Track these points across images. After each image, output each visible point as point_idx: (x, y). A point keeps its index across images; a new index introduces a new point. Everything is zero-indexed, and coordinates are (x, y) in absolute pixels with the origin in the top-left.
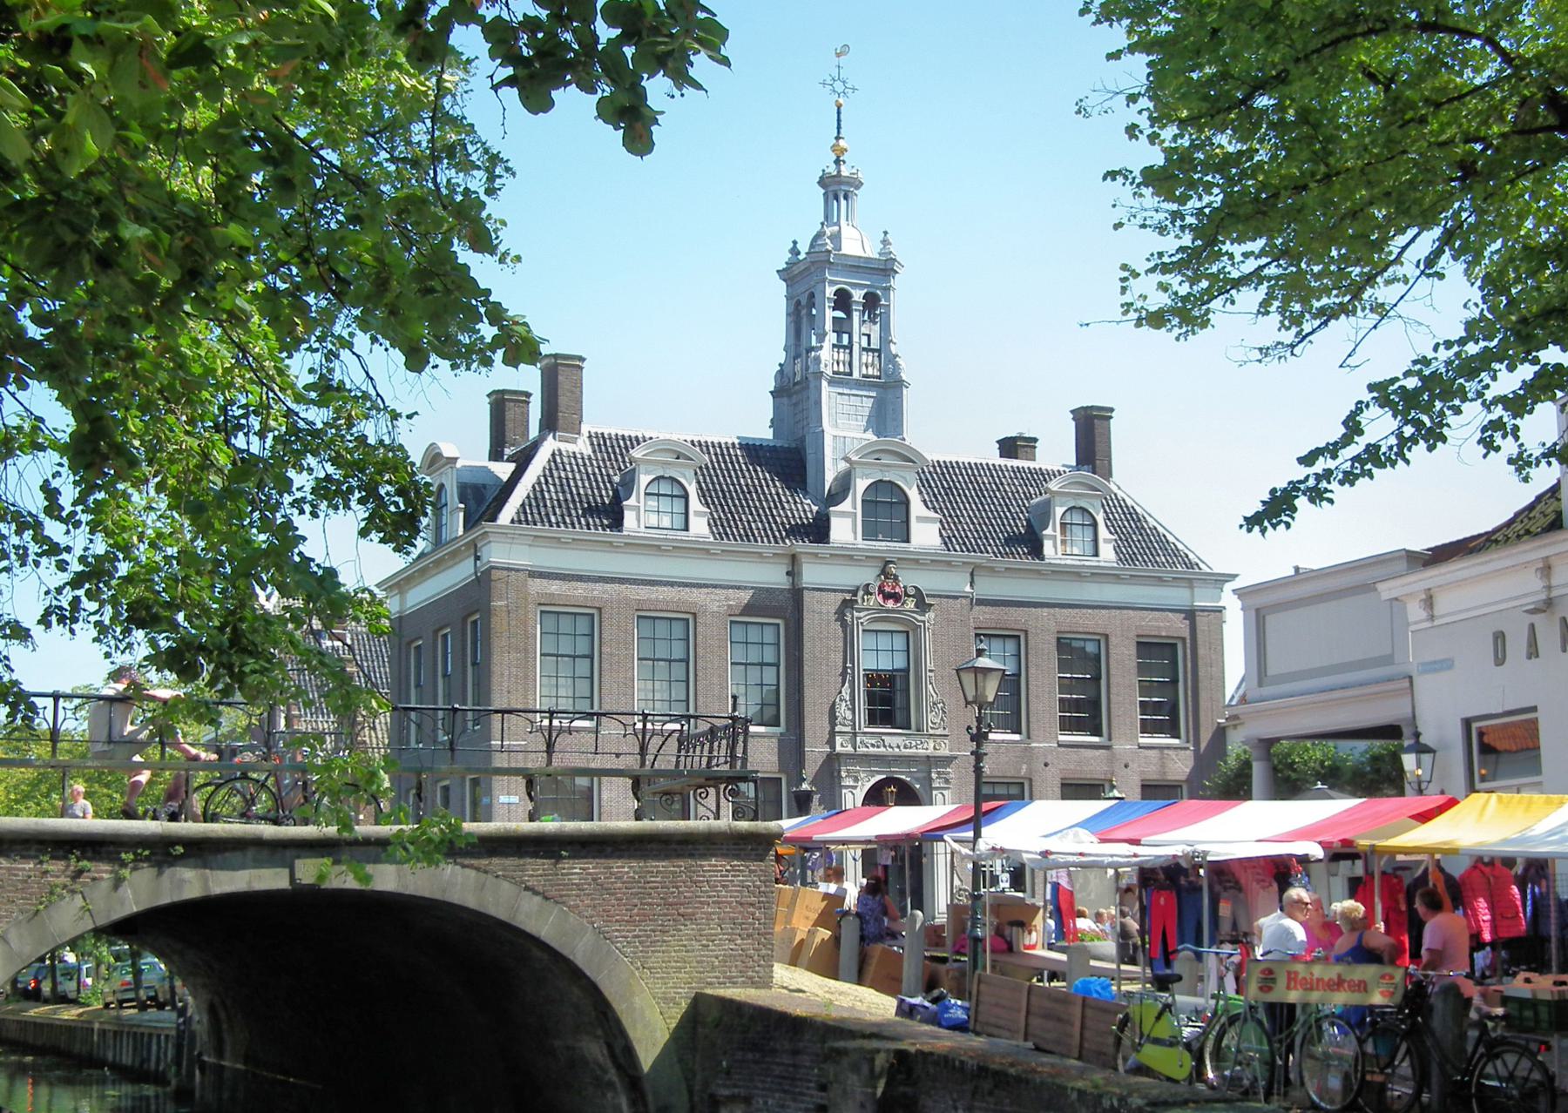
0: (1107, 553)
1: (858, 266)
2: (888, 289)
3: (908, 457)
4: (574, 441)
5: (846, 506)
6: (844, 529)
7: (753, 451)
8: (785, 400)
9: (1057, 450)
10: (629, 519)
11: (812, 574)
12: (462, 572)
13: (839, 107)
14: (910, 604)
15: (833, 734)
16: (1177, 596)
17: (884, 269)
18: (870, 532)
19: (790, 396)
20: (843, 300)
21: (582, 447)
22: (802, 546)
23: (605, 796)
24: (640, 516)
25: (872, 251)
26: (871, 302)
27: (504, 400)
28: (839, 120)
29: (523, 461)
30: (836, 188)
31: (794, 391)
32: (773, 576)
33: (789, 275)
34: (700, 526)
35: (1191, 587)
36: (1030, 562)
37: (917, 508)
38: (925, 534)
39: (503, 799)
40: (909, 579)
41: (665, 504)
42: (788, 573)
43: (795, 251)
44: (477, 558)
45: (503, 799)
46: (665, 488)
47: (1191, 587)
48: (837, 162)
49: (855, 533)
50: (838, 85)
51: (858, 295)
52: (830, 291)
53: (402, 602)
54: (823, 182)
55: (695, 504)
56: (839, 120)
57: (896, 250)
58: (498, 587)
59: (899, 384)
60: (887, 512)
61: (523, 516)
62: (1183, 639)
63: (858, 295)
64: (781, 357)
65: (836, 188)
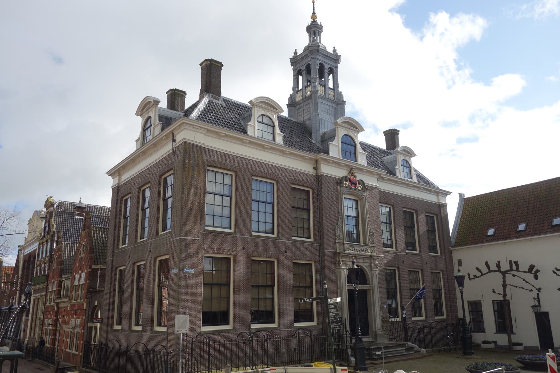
0: (415, 179)
4: (218, 99)
5: (335, 142)
8: (293, 108)
10: (250, 132)
13: (313, 2)
19: (295, 106)
20: (322, 67)
21: (220, 102)
22: (322, 156)
24: (255, 129)
27: (175, 94)
28: (314, 7)
33: (295, 61)
34: (279, 139)
35: (438, 196)
40: (359, 177)
41: (265, 127)
42: (314, 168)
43: (296, 53)
44: (174, 141)
46: (265, 120)
47: (438, 196)
49: (339, 154)
51: (327, 67)
52: (318, 62)
53: (119, 179)
55: (277, 130)
56: (314, 7)
57: (339, 52)
64: (291, 92)
65: (314, 29)
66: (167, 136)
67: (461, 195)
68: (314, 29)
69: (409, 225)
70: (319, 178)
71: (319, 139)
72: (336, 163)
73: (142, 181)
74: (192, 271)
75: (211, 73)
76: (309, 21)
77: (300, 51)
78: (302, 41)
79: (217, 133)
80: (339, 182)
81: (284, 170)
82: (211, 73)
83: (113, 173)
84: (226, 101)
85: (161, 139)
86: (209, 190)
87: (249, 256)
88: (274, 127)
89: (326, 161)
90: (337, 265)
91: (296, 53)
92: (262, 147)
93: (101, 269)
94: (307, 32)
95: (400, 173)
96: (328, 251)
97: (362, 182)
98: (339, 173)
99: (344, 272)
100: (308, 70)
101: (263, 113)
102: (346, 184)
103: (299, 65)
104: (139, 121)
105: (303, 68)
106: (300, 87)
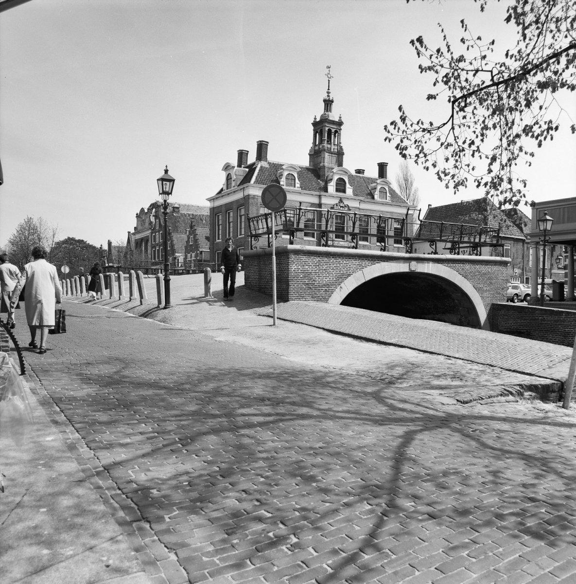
1: (333, 122)
2: (341, 129)
3: (346, 172)
6: (332, 188)
7: (307, 169)
9: (372, 172)
11: (324, 200)
12: (239, 196)
14: (346, 209)
17: (340, 123)
18: (337, 190)
20: (330, 131)
22: (323, 193)
25: (337, 119)
26: (336, 132)
29: (252, 168)
30: (328, 103)
31: (316, 154)
32: (315, 200)
33: (315, 124)
36: (372, 201)
37: (348, 185)
38: (349, 191)
40: (346, 202)
43: (315, 119)
48: (328, 96)
51: (333, 130)
52: (327, 129)
54: (325, 101)
59: (343, 154)
60: (341, 187)
61: (257, 182)
63: (333, 130)
65: (328, 103)
66: (241, 189)
75: (262, 147)
76: (325, 96)
78: (319, 111)
82: (262, 147)
84: (269, 163)
88: (295, 179)
91: (315, 119)
104: (224, 175)
105: (319, 131)
106: (317, 144)
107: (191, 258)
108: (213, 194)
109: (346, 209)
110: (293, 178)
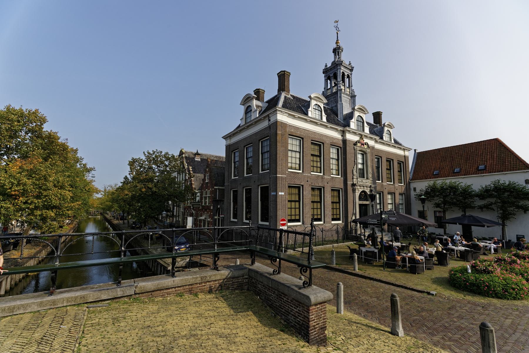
0: (393, 142)
5: (353, 120)
15: (353, 178)
16: (401, 152)
21: (289, 96)
23: (304, 193)
24: (312, 113)
34: (324, 119)
39: (280, 193)
40: (366, 140)
42: (342, 136)
43: (326, 66)
44: (269, 120)
45: (280, 193)
50: (337, 27)
51: (346, 74)
52: (342, 71)
55: (323, 113)
57: (353, 65)
58: (279, 127)
62: (403, 162)
65: (337, 51)
66: (265, 117)
67: (415, 150)
68: (337, 51)
69: (388, 168)
70: (345, 141)
71: (342, 118)
72: (355, 133)
73: (248, 142)
74: (283, 194)
75: (283, 78)
77: (329, 65)
79: (294, 116)
80: (355, 144)
81: (327, 137)
82: (283, 78)
83: (225, 138)
85: (261, 120)
86: (289, 149)
87: (310, 185)
88: (321, 112)
89: (349, 131)
90: (354, 191)
91: (326, 66)
92: (316, 124)
93: (219, 189)
94: (333, 52)
95: (386, 137)
96: (349, 183)
97: (366, 144)
98: (356, 138)
99: (357, 194)
100: (335, 77)
101: (316, 103)
102: (359, 144)
103: (329, 73)
106: (329, 87)
107: (206, 194)
108: (232, 128)
109: (366, 146)
110: (320, 109)
